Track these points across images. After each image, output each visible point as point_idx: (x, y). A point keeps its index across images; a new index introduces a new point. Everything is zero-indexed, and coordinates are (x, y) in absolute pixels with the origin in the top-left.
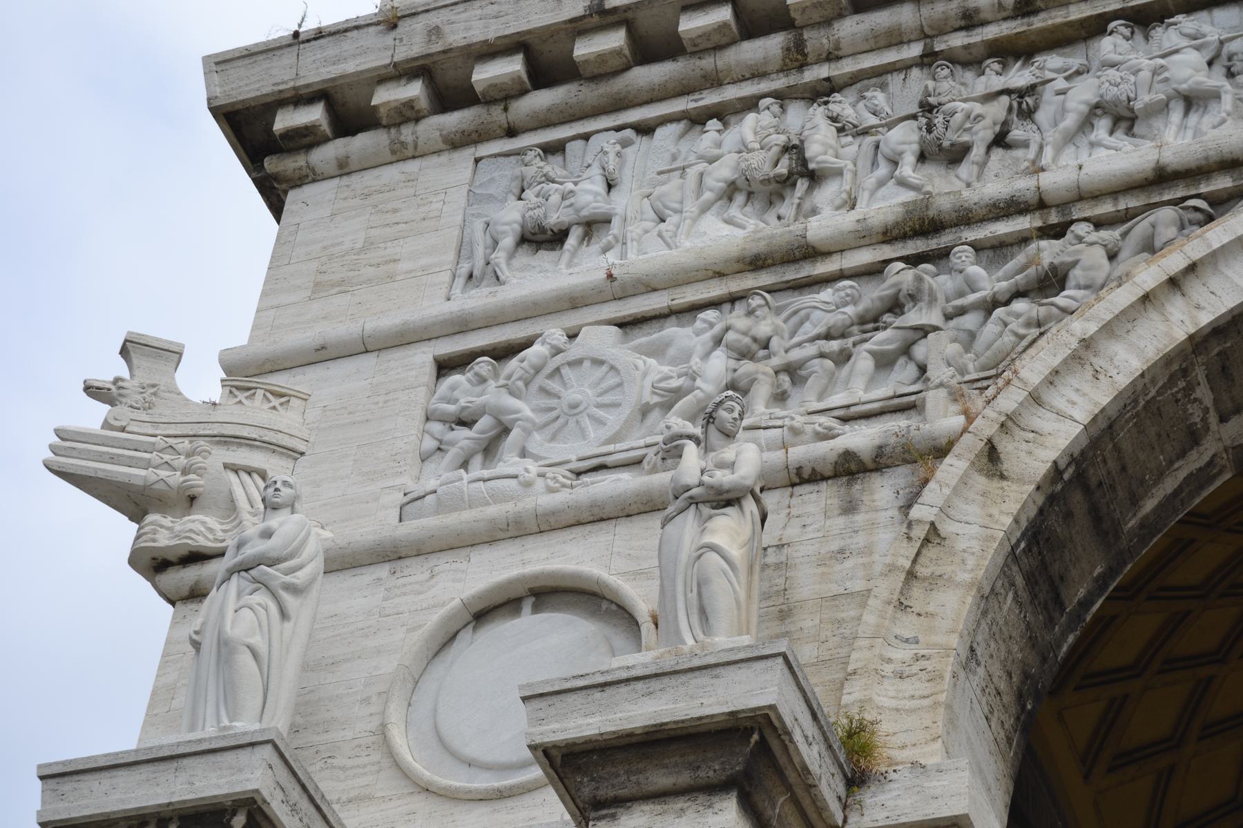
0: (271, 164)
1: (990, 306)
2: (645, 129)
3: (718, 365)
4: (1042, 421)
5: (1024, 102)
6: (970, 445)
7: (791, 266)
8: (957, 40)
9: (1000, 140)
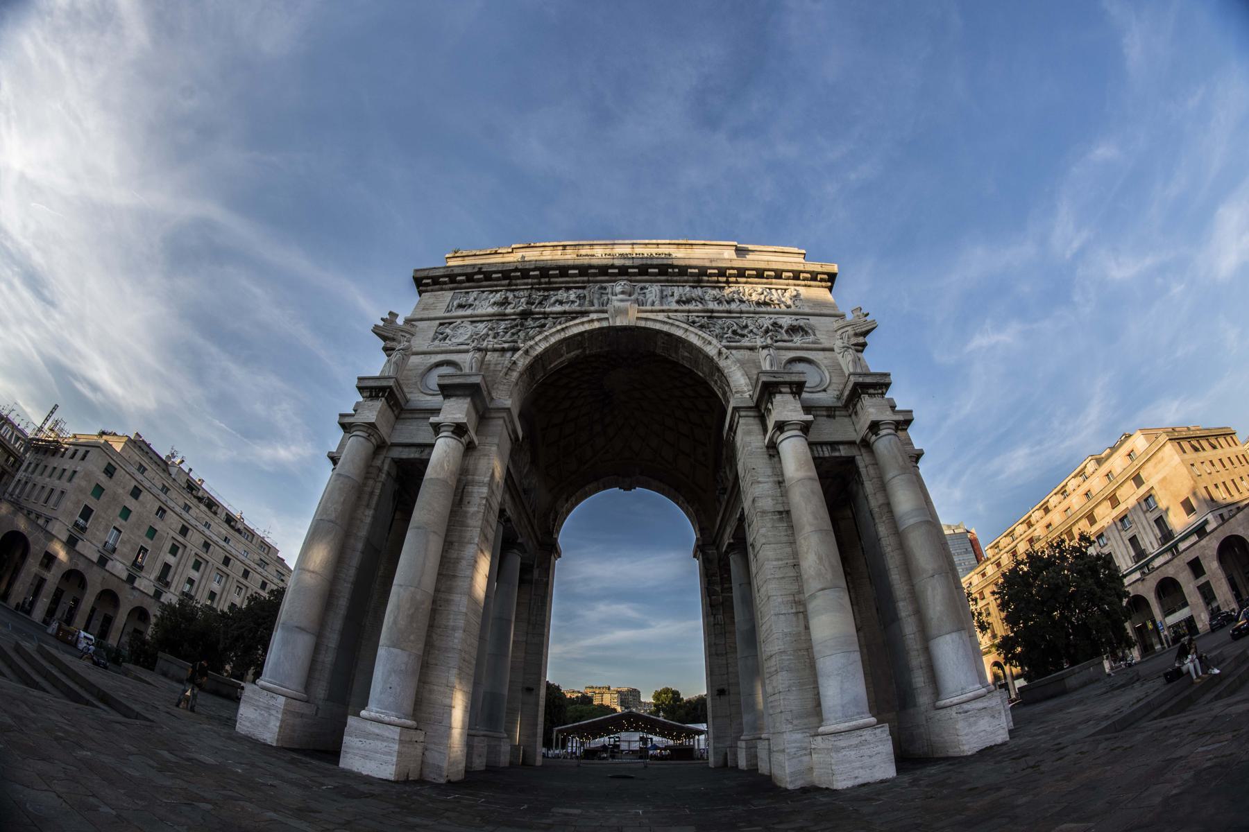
5: (546, 298)
7: (502, 316)
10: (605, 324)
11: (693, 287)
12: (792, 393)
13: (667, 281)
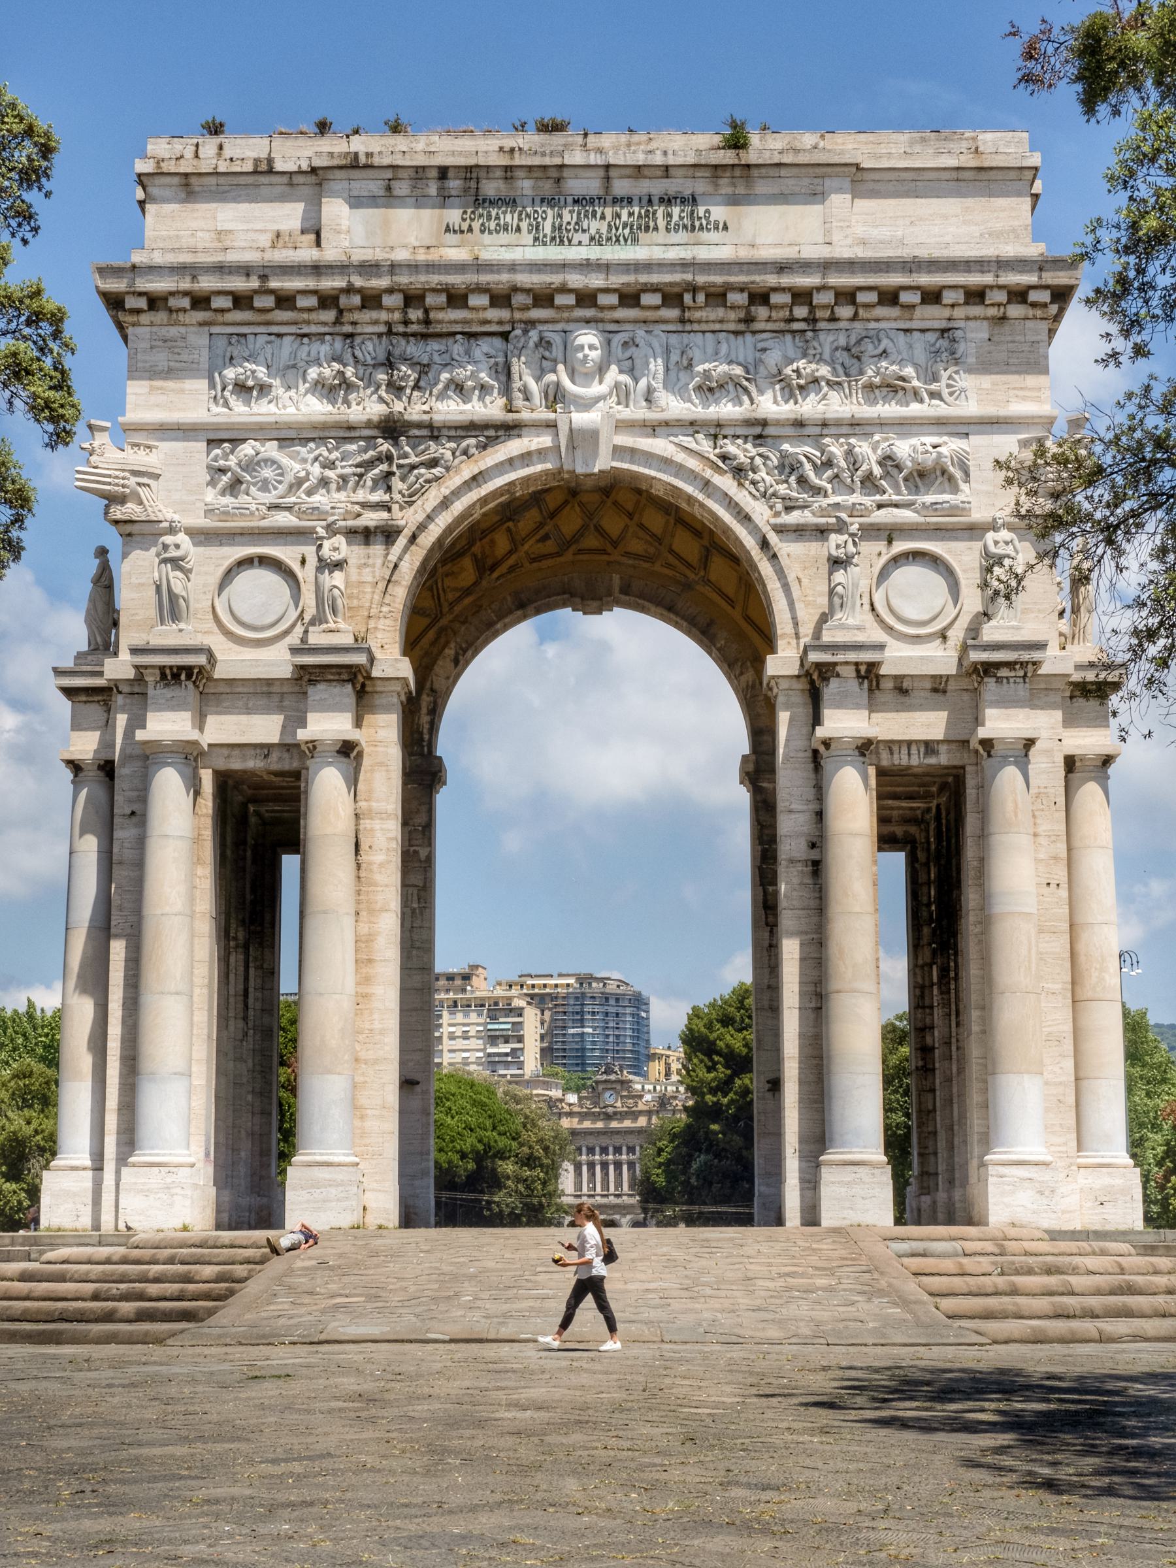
0: (122, 316)
1: (413, 467)
3: (316, 470)
9: (416, 387)
11: (736, 333)
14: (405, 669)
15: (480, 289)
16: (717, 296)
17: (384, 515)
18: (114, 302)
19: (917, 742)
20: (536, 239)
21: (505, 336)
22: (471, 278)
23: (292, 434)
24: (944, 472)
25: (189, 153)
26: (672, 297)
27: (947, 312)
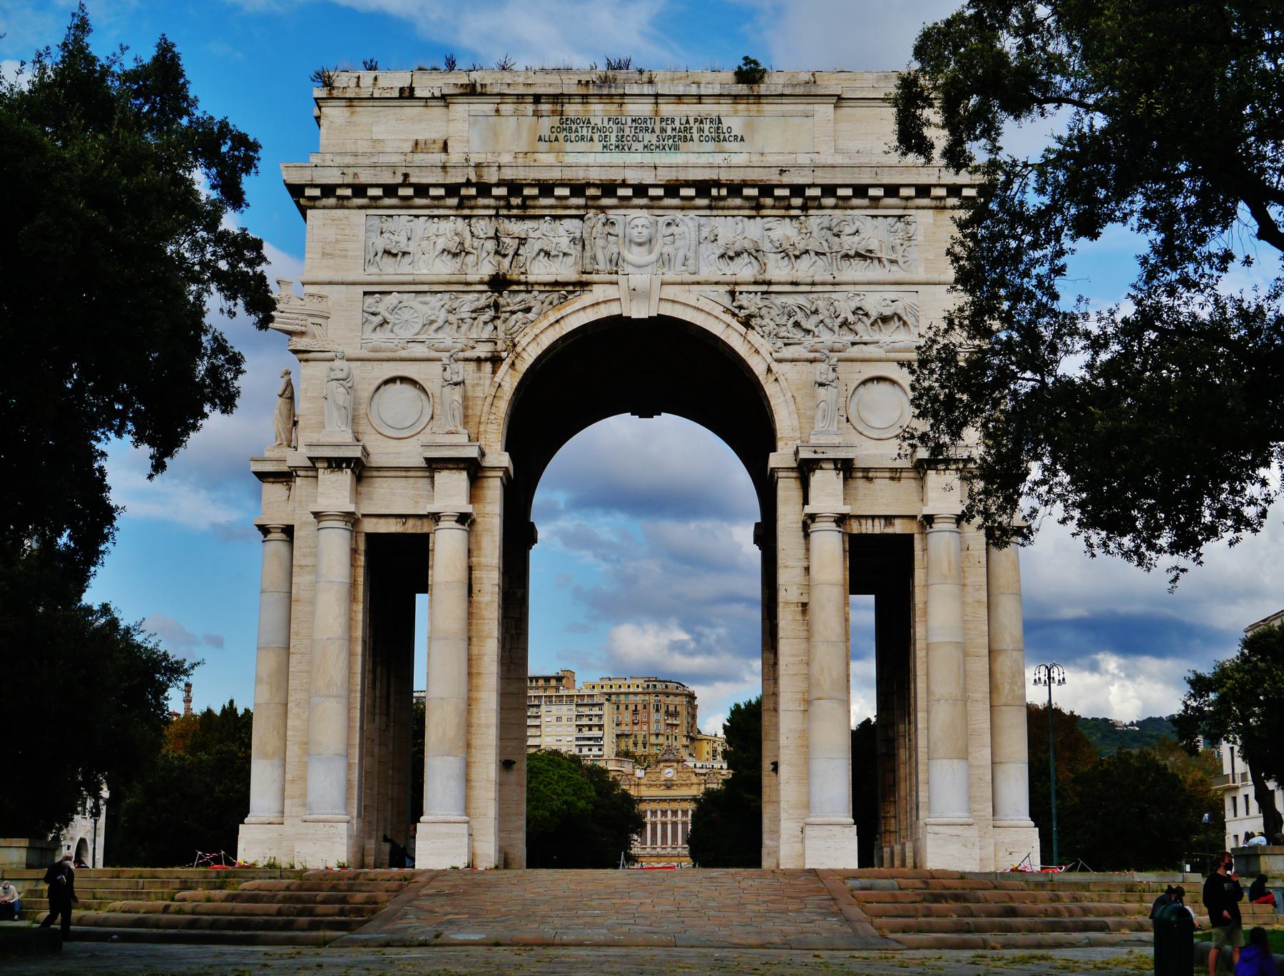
0: (302, 201)
1: (513, 313)
2: (417, 216)
3: (443, 315)
4: (524, 355)
5: (523, 241)
6: (508, 361)
8: (504, 212)
10: (614, 310)
11: (749, 217)
12: (836, 469)
13: (710, 207)
14: (504, 460)
15: (562, 184)
16: (735, 189)
17: (490, 347)
18: (296, 190)
19: (879, 517)
20: (604, 147)
21: (581, 217)
22: (555, 175)
23: (425, 288)
24: (900, 318)
25: (353, 83)
26: (703, 188)
27: (903, 203)
